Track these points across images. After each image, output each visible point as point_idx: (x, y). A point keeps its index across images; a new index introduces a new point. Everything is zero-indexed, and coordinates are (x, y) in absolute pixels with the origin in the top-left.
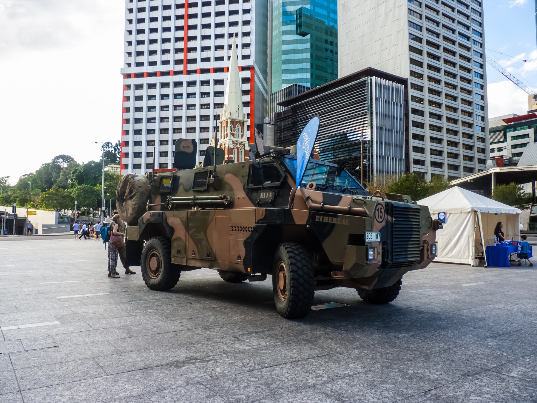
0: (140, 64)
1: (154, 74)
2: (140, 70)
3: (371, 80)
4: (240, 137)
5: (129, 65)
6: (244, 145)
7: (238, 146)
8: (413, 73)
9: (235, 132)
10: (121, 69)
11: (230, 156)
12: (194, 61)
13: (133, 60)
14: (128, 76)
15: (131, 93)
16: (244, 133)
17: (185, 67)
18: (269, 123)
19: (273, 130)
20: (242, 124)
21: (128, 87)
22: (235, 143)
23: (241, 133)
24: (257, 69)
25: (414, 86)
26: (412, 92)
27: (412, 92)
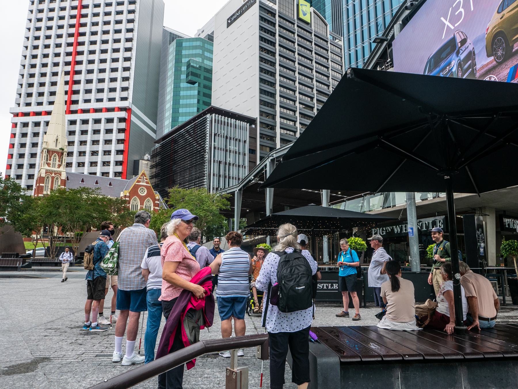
0: (28, 104)
3: (212, 117)
4: (57, 166)
5: (19, 104)
6: (60, 175)
7: (53, 175)
9: (51, 162)
11: (41, 185)
14: (16, 115)
15: (18, 131)
16: (62, 163)
18: (147, 160)
19: (149, 166)
20: (61, 153)
22: (47, 172)
23: (57, 163)
24: (135, 109)
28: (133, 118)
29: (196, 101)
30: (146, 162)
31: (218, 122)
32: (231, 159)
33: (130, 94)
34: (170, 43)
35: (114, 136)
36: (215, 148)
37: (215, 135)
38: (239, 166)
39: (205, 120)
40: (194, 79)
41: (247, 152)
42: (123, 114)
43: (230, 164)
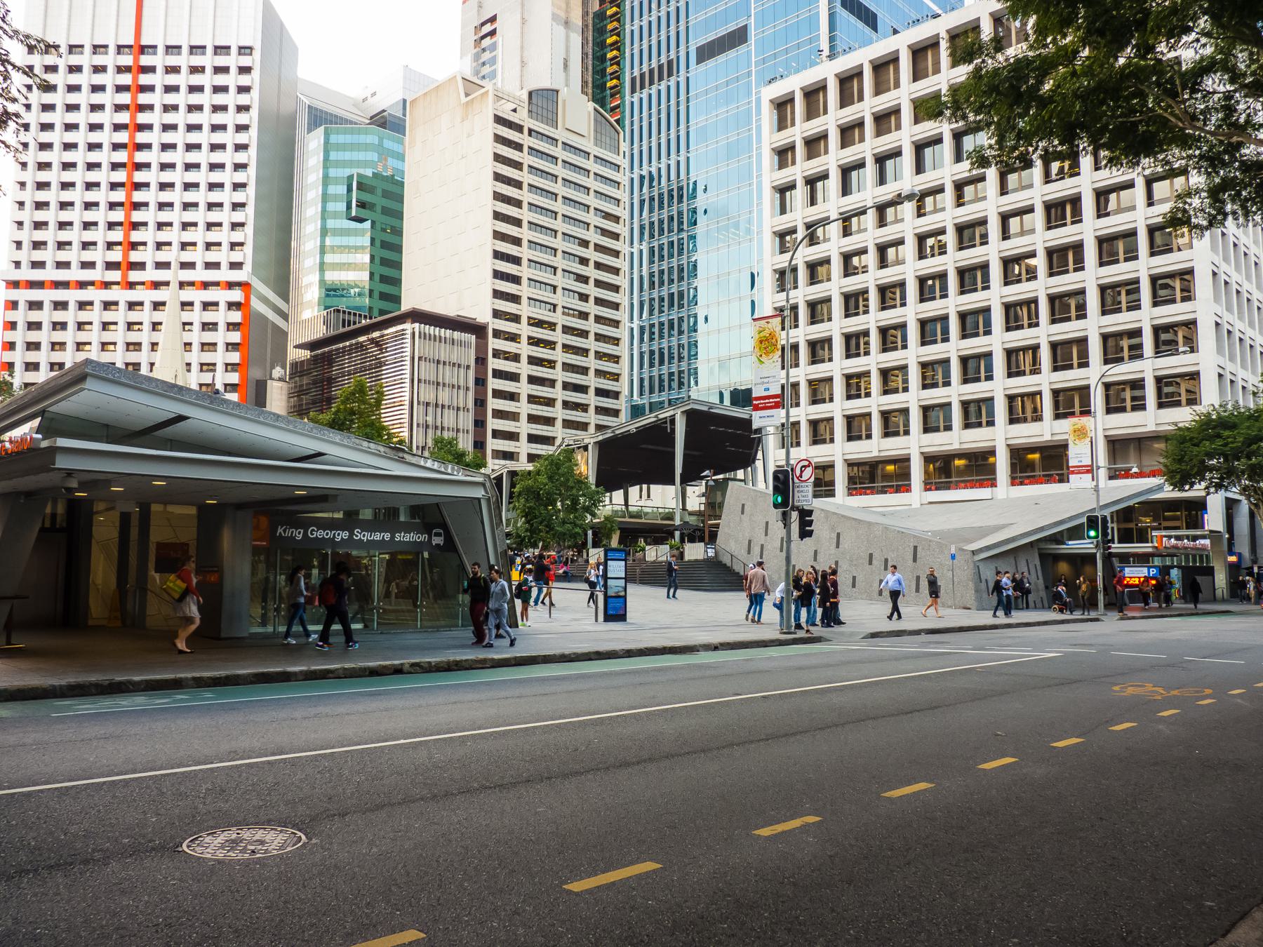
1: (64, 285)
2: (37, 275)
5: (18, 264)
8: (497, 314)
12: (141, 266)
13: (25, 255)
14: (15, 284)
15: (20, 316)
17: (125, 276)
18: (280, 379)
19: (285, 392)
21: (13, 305)
24: (258, 285)
25: (497, 334)
26: (493, 343)
29: (367, 259)
30: (280, 384)
31: (423, 336)
32: (444, 396)
33: (246, 254)
34: (310, 131)
35: (221, 337)
36: (419, 381)
37: (420, 358)
38: (458, 409)
39: (402, 333)
40: (363, 213)
41: (471, 384)
42: (237, 295)
43: (443, 406)
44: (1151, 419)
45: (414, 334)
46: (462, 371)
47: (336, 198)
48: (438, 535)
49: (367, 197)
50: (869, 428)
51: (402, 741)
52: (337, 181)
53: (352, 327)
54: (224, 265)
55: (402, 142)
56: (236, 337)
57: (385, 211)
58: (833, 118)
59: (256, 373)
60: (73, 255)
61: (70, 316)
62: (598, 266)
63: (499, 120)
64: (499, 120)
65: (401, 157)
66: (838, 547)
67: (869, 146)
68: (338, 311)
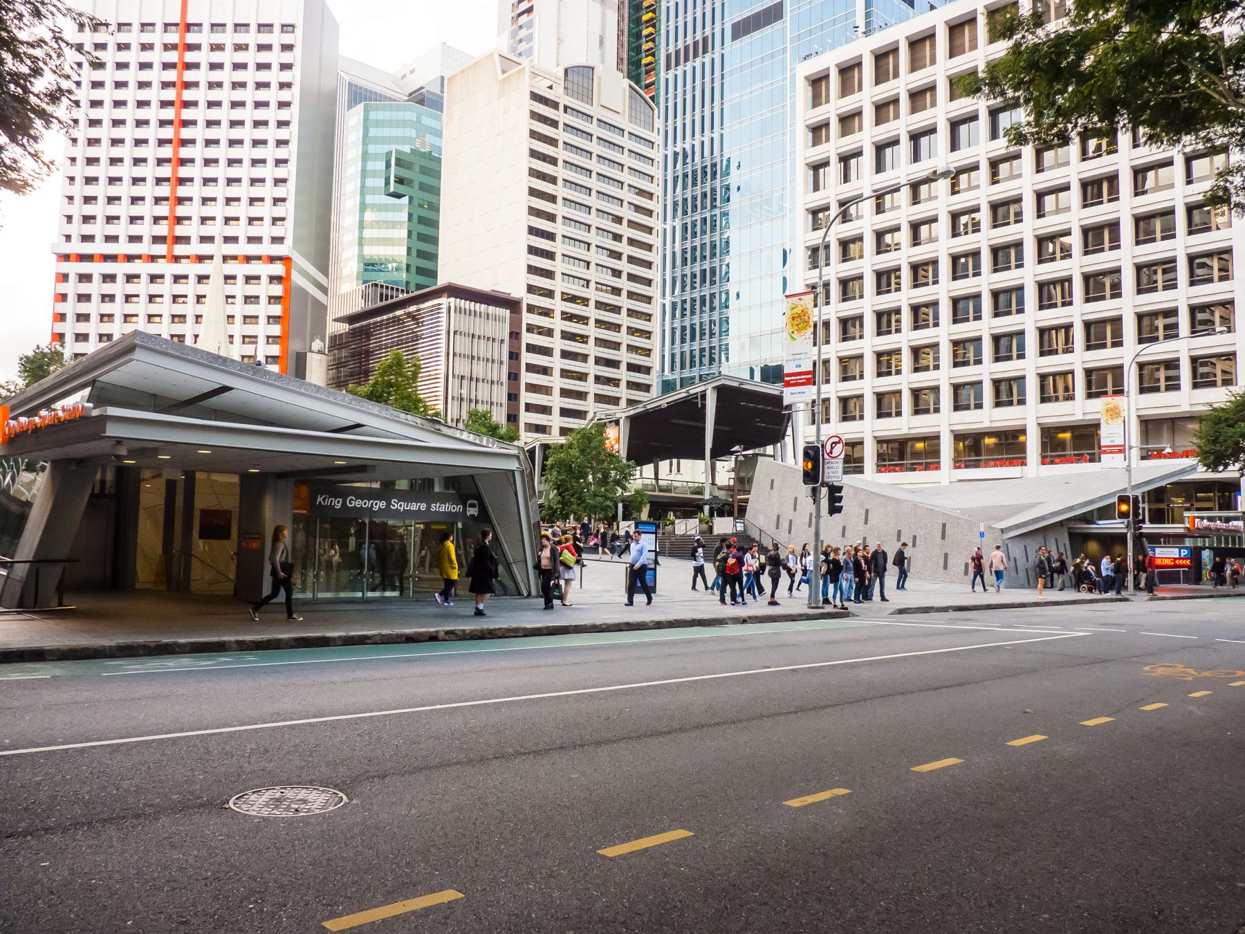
1: (112, 258)
2: (87, 248)
5: (68, 238)
8: (531, 289)
10: (53, 245)
12: (185, 240)
13: (77, 229)
14: (66, 258)
15: (72, 288)
17: (170, 250)
18: (319, 352)
19: (324, 364)
21: (64, 277)
24: (298, 259)
25: (531, 309)
26: (528, 318)
27: (528, 318)
28: (297, 278)
29: (404, 233)
30: (320, 356)
31: (460, 311)
32: (479, 370)
33: (287, 229)
34: (350, 107)
35: (263, 309)
36: (454, 354)
37: (455, 332)
38: (492, 382)
40: (401, 189)
42: (278, 269)
43: (477, 380)
44: (1187, 399)
45: (449, 308)
46: (496, 344)
47: (375, 174)
48: (472, 506)
49: (404, 173)
50: (899, 405)
51: (438, 707)
52: (376, 157)
53: (390, 301)
54: (266, 240)
55: (439, 119)
56: (277, 310)
57: (424, 187)
58: (868, 95)
59: (295, 346)
60: (122, 229)
61: (119, 288)
62: (632, 242)
63: (535, 97)
64: (535, 97)
65: (438, 133)
66: (866, 523)
67: (904, 123)
68: (376, 285)
